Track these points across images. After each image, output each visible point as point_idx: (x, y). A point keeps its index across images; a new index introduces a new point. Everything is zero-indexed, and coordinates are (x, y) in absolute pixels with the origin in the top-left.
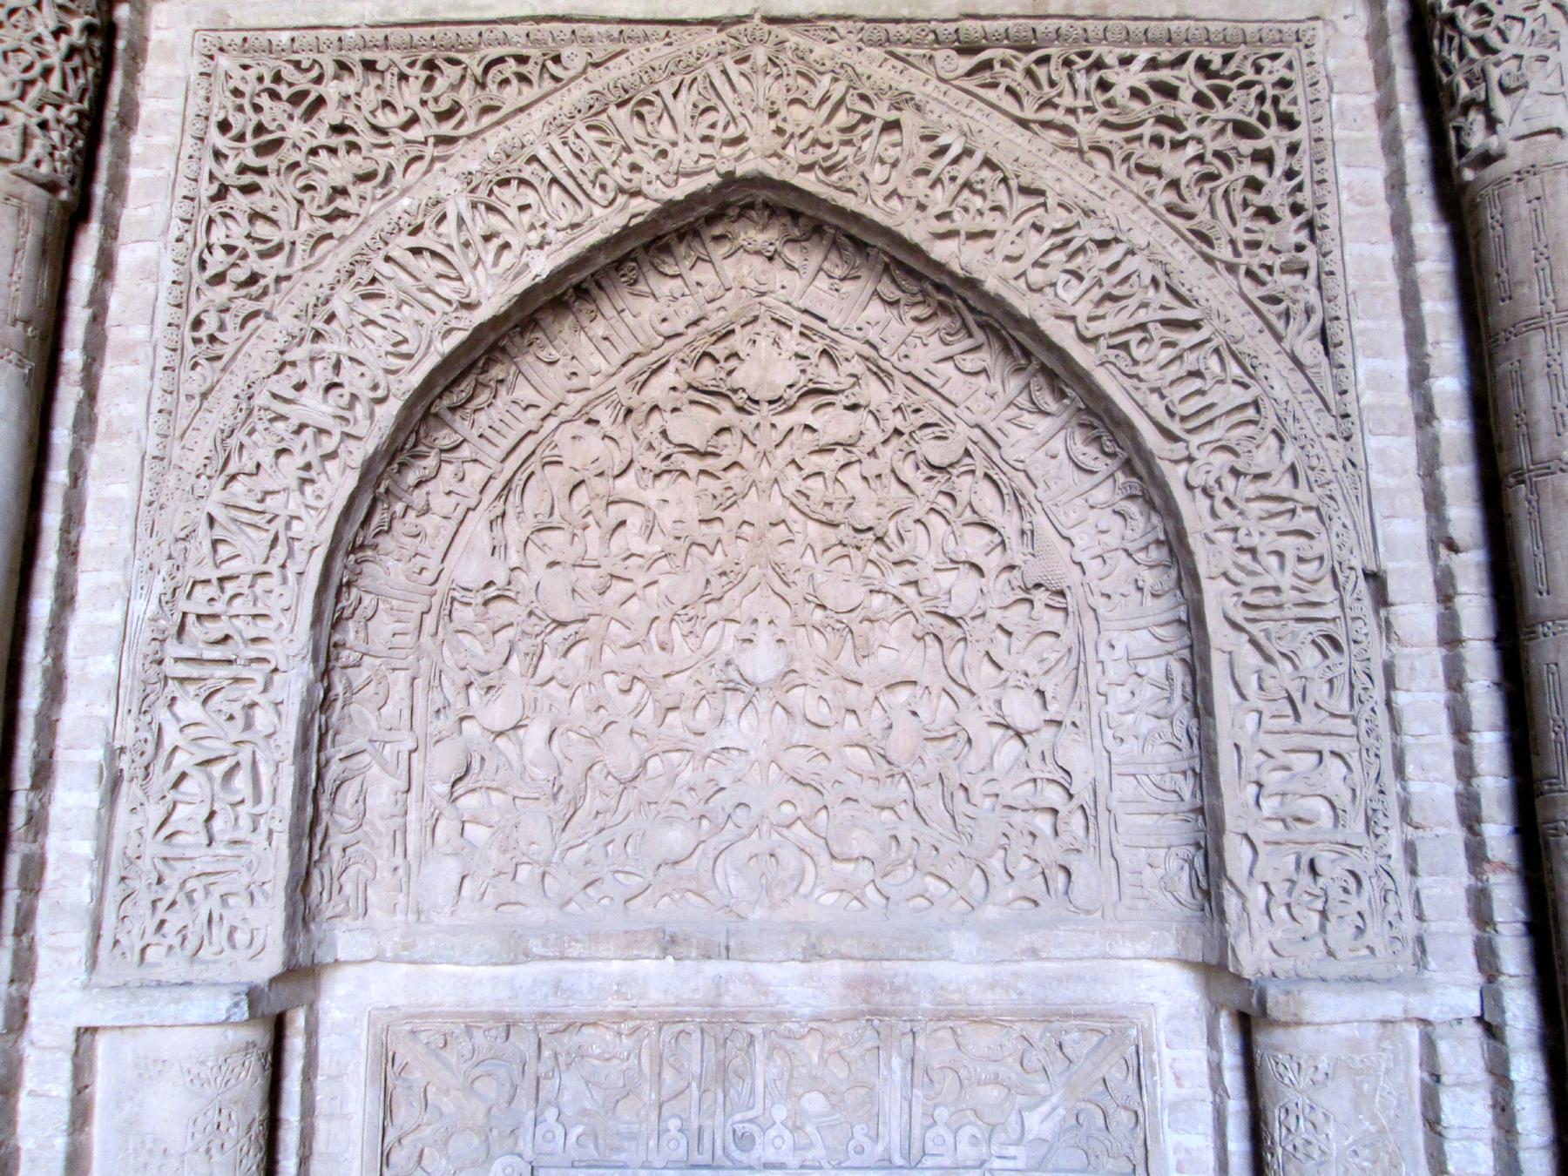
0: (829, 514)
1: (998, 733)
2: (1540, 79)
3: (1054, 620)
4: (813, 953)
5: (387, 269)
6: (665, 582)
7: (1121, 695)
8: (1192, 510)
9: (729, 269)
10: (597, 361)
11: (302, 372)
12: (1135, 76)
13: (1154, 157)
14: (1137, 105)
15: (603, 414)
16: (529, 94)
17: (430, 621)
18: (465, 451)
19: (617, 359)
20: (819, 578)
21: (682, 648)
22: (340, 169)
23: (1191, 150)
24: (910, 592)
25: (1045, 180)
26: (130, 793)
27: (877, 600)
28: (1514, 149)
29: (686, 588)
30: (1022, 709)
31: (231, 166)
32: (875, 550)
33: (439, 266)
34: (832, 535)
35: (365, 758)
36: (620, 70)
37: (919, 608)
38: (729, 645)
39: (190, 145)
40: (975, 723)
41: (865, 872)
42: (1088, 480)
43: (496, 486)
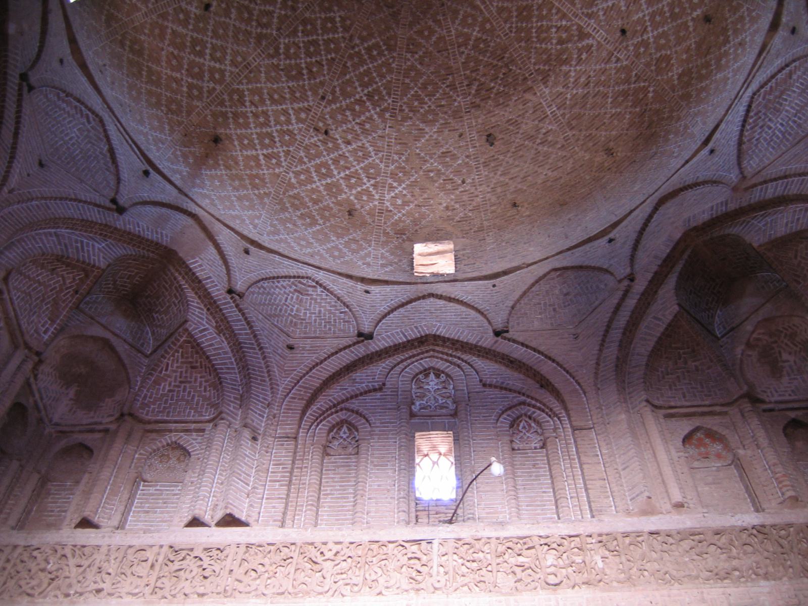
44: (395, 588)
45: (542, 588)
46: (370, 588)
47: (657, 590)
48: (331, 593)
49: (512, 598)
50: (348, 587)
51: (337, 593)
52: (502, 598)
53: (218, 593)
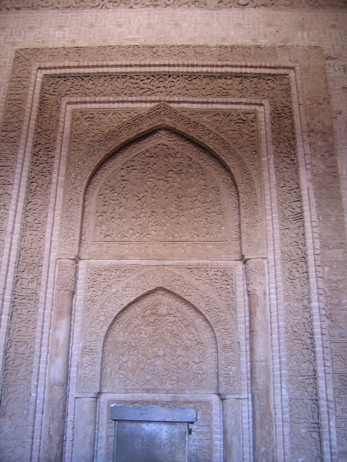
0: (171, 332)
1: (194, 363)
2: (254, 284)
3: (202, 348)
4: (167, 393)
5: (112, 299)
6: (148, 341)
7: (210, 358)
8: (218, 334)
9: (157, 297)
10: (139, 310)
11: (100, 314)
12: (212, 273)
13: (214, 284)
14: (212, 277)
15: (139, 317)
16: (130, 274)
17: (115, 346)
18: (120, 322)
19: (141, 309)
20: (169, 341)
21: (150, 351)
22: (104, 285)
23: (219, 284)
24: (182, 343)
25: (199, 288)
26: (80, 368)
27: (177, 344)
28: (252, 291)
29: (151, 343)
30: (196, 360)
31: (90, 284)
32: (177, 337)
33: (118, 299)
34: (171, 335)
35: (106, 365)
36: (143, 272)
37: (183, 345)
38: (157, 350)
39: (85, 282)
40: (190, 362)
41: (175, 382)
42: (206, 328)
43: (124, 327)
44: (141, 4)
45: (235, 7)
46: (125, 4)
47: (309, 11)
48: (100, 7)
49: (215, 12)
50: (111, 4)
51: (104, 7)
52: (209, 12)
53: (29, 7)
